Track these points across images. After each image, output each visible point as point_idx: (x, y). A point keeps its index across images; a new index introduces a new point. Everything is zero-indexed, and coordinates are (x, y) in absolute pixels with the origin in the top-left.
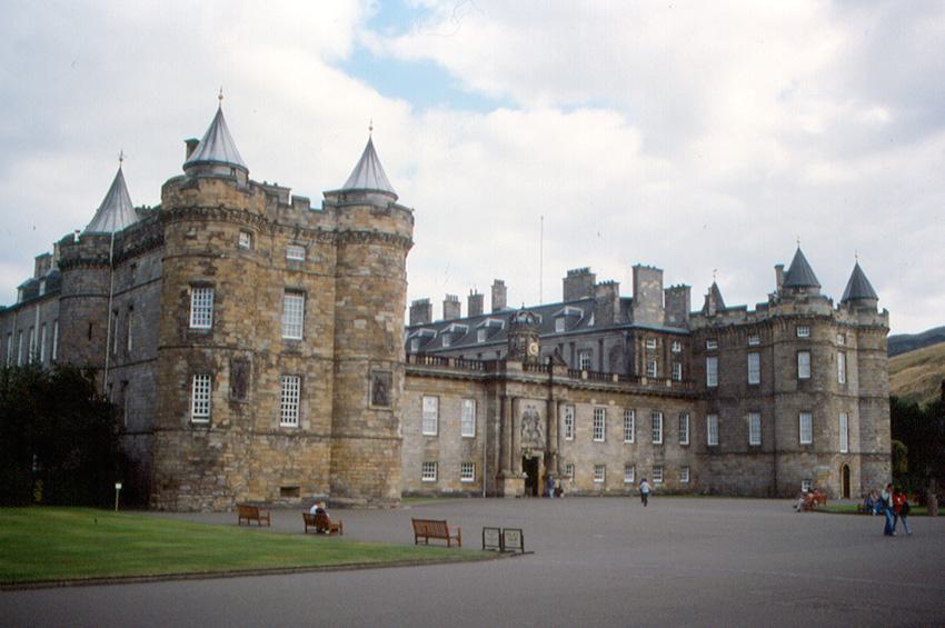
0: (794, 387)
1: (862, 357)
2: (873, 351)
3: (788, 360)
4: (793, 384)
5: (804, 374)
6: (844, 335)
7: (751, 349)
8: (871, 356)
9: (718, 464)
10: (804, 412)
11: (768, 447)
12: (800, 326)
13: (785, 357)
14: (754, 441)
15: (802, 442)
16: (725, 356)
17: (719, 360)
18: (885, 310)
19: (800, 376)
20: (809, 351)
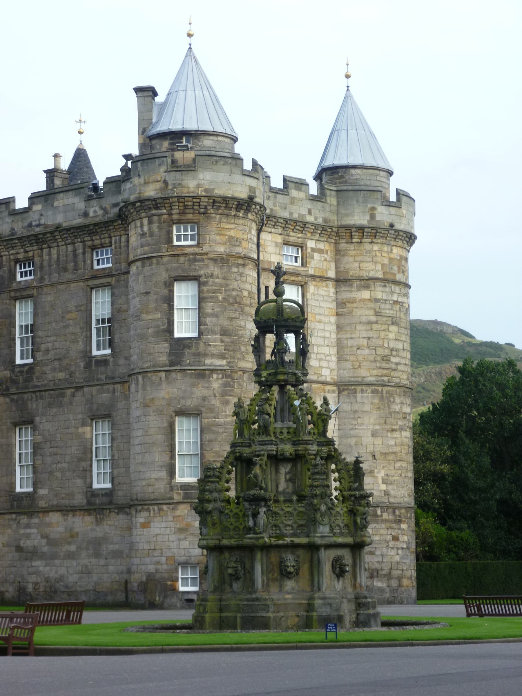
0: (163, 359)
1: (345, 295)
2: (367, 282)
3: (152, 297)
4: (161, 352)
5: (184, 327)
6: (302, 247)
7: (98, 280)
8: (366, 294)
9: (33, 536)
10: (180, 413)
11: (120, 497)
12: (179, 222)
13: (147, 293)
14: (100, 483)
15: (179, 479)
16: (48, 297)
17: (35, 308)
18: (399, 193)
19: (177, 335)
20: (195, 278)
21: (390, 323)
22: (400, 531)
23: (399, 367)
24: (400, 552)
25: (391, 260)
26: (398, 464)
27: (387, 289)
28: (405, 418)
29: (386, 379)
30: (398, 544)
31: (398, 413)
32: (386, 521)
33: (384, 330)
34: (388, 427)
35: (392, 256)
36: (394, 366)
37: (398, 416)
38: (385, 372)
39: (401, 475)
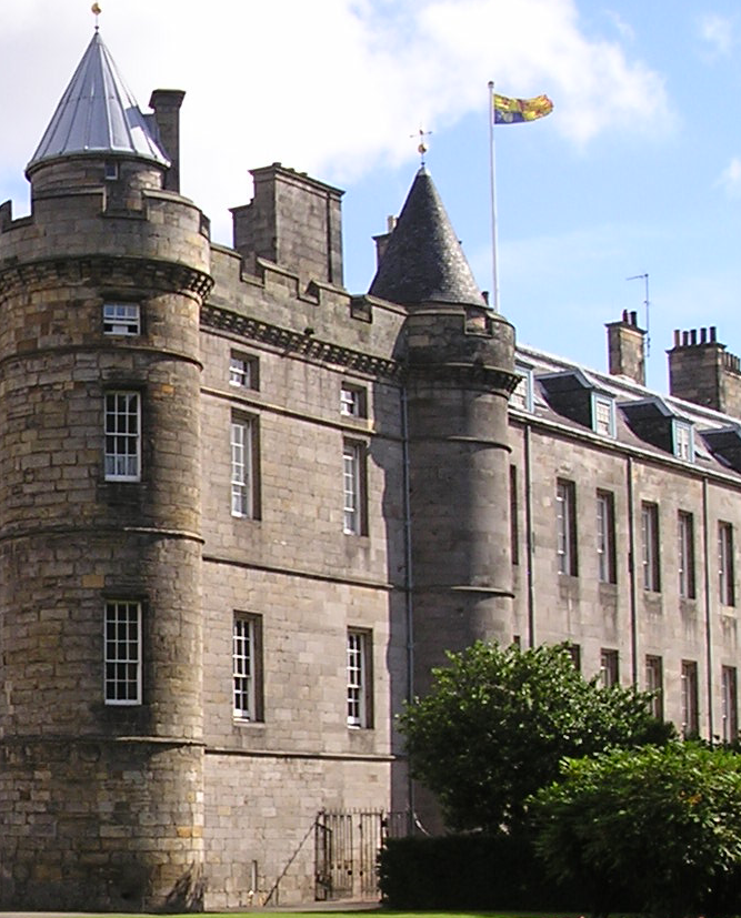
21: (22, 427)
22: (32, 784)
23: (39, 500)
24: (32, 819)
25: (28, 316)
26: (32, 669)
27: (20, 371)
28: (50, 587)
29: (15, 525)
30: (29, 806)
31: (33, 579)
32: (13, 767)
33: (15, 443)
34: (17, 607)
35: (31, 310)
36: (28, 500)
37: (33, 585)
38: (16, 513)
39: (36, 687)
